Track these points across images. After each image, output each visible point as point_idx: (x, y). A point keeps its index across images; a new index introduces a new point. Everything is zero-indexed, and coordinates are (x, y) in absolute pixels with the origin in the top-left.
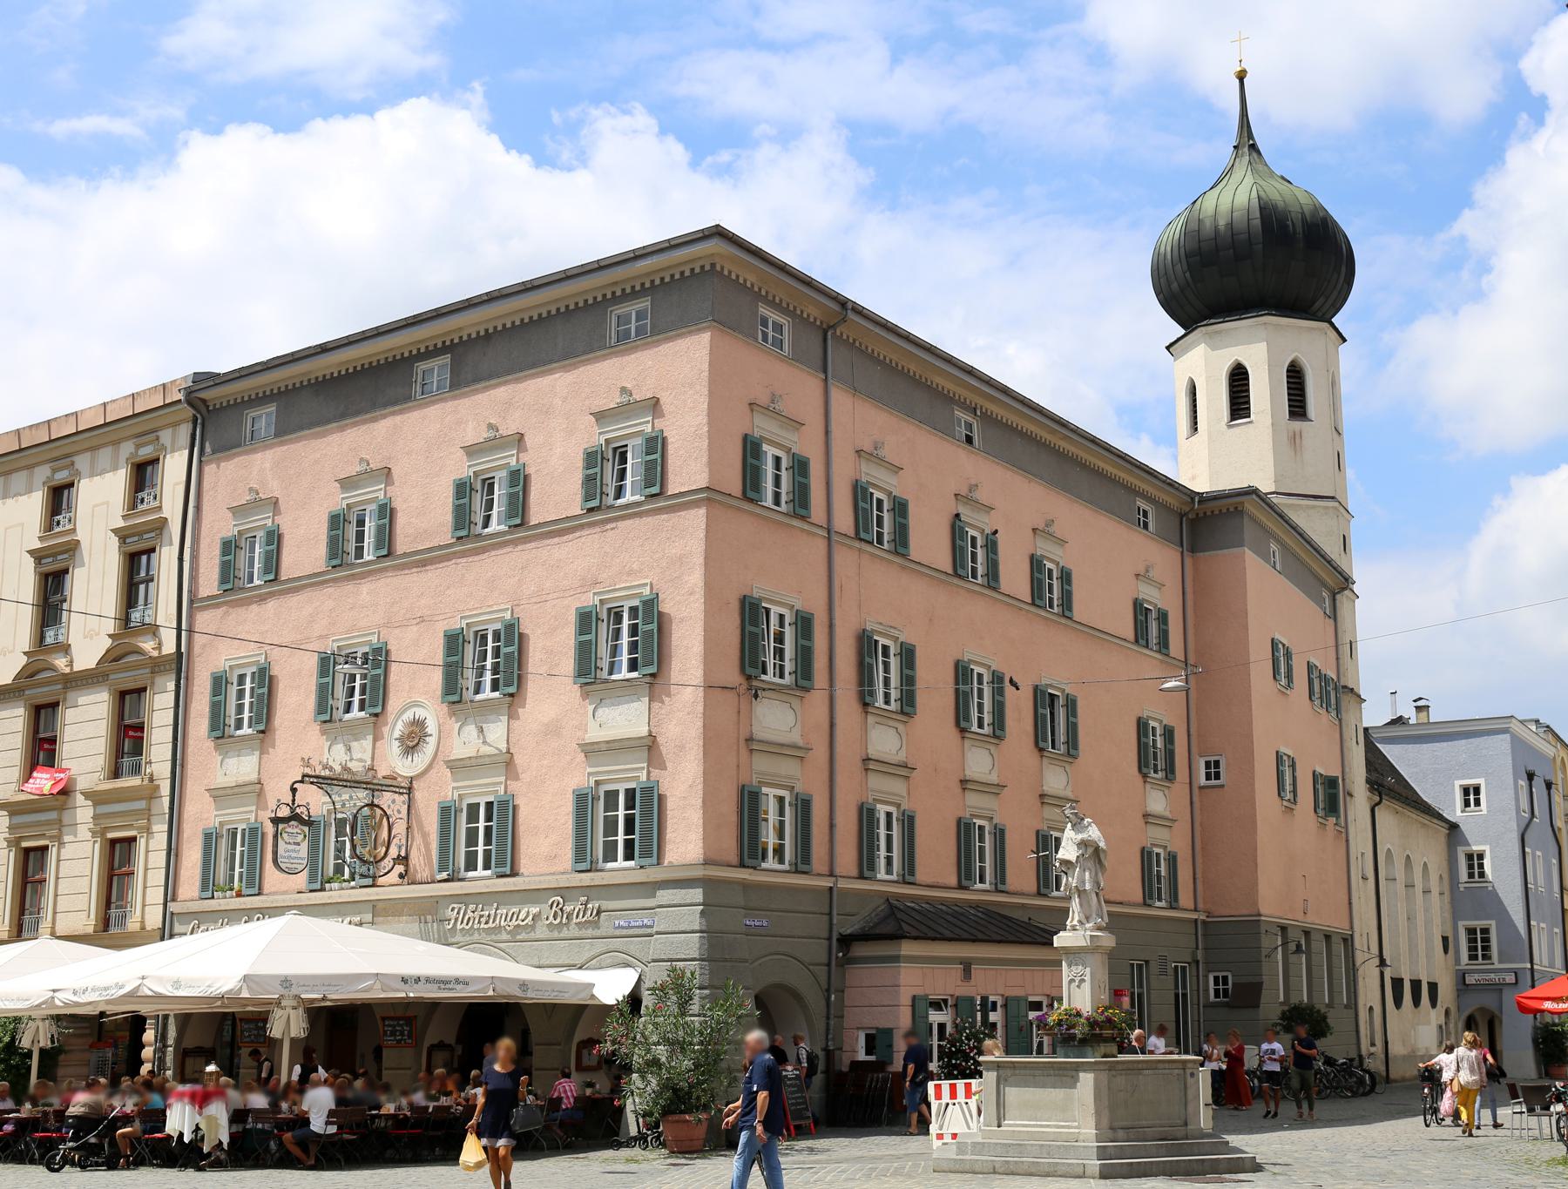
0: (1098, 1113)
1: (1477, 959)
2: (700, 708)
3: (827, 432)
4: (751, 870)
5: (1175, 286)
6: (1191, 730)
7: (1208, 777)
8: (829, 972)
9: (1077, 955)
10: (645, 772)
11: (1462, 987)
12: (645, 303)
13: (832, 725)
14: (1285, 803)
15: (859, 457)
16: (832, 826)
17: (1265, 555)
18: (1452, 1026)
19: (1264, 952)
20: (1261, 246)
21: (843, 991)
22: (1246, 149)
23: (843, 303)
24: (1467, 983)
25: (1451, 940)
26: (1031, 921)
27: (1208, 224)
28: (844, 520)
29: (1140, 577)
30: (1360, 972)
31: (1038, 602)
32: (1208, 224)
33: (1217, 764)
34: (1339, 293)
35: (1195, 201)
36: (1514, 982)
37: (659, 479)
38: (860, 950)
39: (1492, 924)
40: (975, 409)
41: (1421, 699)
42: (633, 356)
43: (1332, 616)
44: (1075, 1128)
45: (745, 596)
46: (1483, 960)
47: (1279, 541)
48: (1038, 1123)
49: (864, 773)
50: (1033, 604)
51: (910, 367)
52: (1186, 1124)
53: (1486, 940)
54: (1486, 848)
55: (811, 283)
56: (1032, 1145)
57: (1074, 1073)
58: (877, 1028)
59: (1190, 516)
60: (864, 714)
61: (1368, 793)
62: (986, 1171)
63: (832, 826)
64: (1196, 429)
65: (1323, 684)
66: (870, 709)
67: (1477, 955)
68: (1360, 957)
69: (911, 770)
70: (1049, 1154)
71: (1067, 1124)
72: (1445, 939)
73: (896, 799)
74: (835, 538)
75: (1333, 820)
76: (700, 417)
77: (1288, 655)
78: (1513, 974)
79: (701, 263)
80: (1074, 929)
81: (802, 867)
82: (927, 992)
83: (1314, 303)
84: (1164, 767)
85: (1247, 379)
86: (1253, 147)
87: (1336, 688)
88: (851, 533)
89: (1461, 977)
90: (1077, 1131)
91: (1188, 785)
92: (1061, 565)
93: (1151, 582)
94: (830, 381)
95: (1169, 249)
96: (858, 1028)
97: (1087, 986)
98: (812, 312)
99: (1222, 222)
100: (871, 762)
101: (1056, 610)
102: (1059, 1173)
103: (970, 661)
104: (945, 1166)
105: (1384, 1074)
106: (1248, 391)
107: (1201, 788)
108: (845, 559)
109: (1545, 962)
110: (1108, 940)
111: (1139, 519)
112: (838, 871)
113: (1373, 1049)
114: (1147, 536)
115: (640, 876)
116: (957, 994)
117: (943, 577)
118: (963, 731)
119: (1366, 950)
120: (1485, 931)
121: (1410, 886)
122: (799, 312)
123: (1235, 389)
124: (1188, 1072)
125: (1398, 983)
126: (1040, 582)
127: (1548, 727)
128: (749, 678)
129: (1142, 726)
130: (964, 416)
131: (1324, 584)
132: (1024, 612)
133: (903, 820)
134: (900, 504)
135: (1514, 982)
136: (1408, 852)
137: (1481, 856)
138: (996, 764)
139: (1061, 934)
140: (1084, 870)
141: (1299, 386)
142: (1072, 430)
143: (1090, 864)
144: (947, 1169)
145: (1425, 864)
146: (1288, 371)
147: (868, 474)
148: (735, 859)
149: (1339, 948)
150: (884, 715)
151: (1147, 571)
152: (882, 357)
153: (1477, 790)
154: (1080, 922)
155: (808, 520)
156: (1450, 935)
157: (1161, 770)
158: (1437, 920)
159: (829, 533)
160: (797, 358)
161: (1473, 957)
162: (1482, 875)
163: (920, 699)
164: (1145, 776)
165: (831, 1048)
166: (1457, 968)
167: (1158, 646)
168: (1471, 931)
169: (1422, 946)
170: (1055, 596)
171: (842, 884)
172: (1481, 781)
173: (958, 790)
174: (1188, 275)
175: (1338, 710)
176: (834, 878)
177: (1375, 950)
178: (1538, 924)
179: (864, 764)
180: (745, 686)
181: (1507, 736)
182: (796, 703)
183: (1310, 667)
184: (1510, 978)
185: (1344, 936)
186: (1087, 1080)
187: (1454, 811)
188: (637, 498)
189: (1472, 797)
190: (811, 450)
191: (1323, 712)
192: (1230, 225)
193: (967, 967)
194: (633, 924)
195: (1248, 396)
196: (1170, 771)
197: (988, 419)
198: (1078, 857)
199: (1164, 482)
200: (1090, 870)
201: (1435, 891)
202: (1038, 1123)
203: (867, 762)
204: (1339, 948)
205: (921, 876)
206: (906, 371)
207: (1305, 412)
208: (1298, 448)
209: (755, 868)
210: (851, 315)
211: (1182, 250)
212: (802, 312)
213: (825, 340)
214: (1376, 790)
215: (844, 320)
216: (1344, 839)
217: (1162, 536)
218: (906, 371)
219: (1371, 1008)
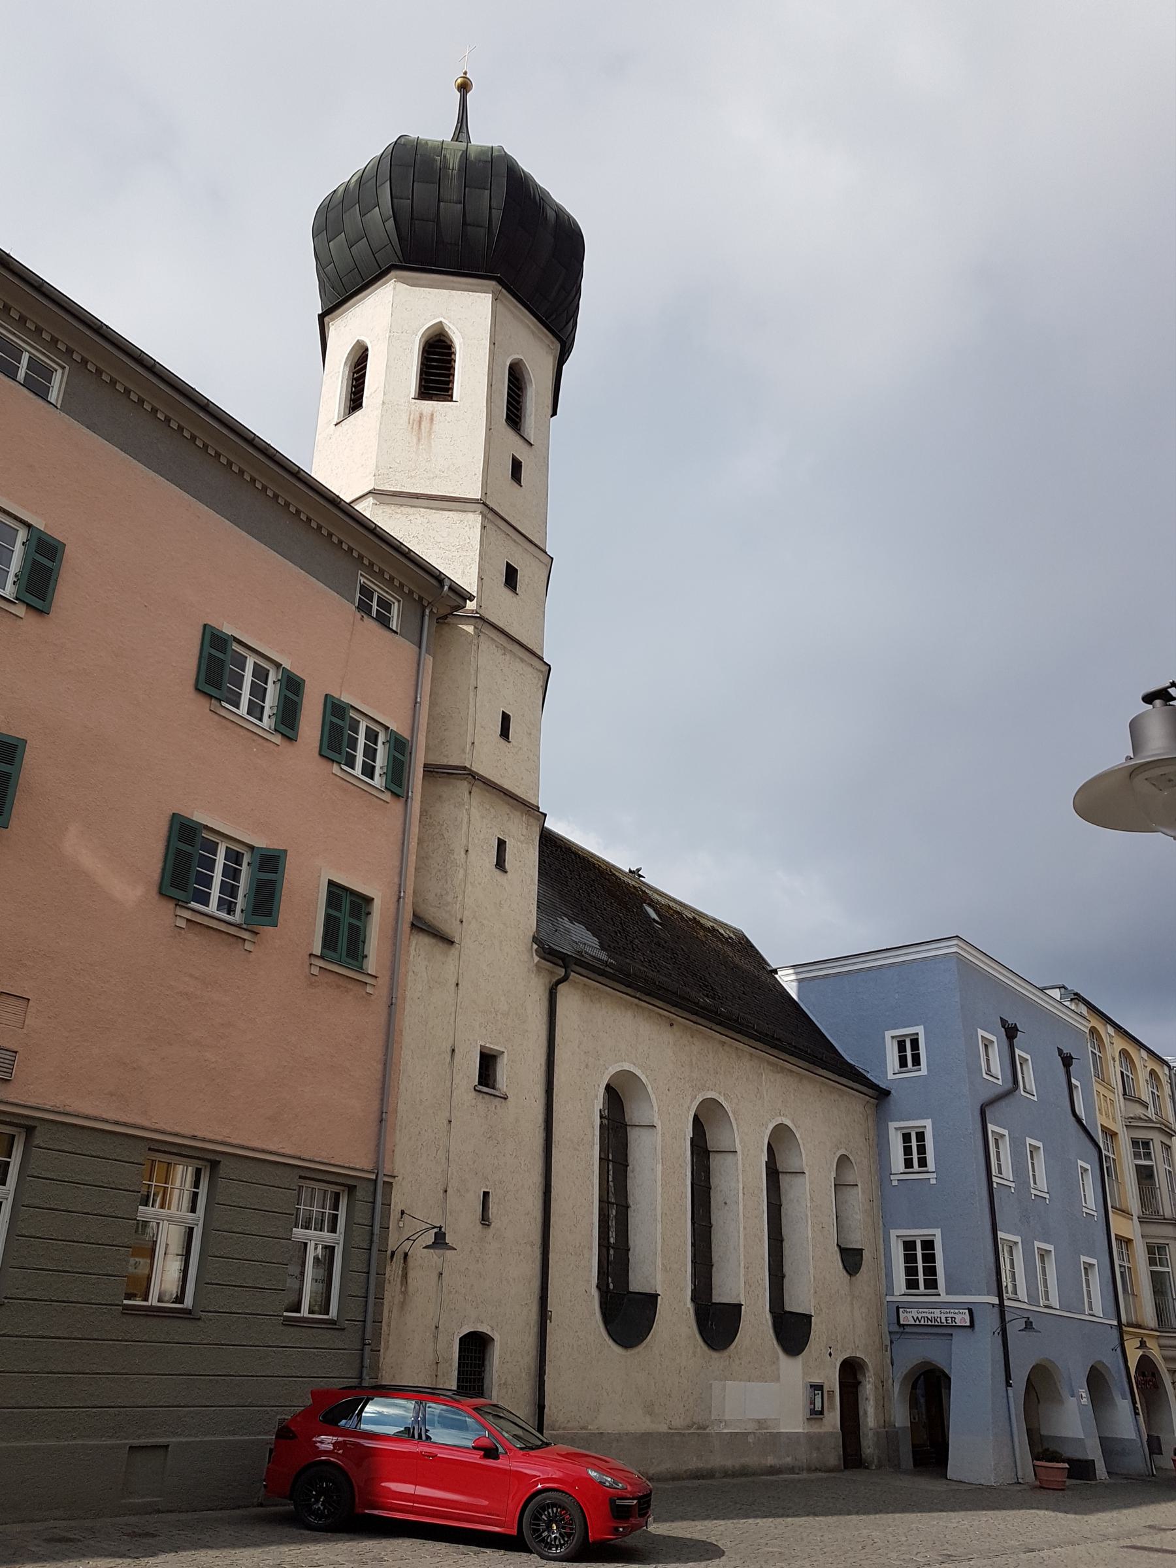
11: (896, 1328)
24: (902, 1322)
53: (929, 1258)
61: (536, 959)
109: (1022, 1294)
120: (928, 1245)
161: (912, 1284)
162: (923, 1162)
166: (889, 1298)
168: (909, 1245)
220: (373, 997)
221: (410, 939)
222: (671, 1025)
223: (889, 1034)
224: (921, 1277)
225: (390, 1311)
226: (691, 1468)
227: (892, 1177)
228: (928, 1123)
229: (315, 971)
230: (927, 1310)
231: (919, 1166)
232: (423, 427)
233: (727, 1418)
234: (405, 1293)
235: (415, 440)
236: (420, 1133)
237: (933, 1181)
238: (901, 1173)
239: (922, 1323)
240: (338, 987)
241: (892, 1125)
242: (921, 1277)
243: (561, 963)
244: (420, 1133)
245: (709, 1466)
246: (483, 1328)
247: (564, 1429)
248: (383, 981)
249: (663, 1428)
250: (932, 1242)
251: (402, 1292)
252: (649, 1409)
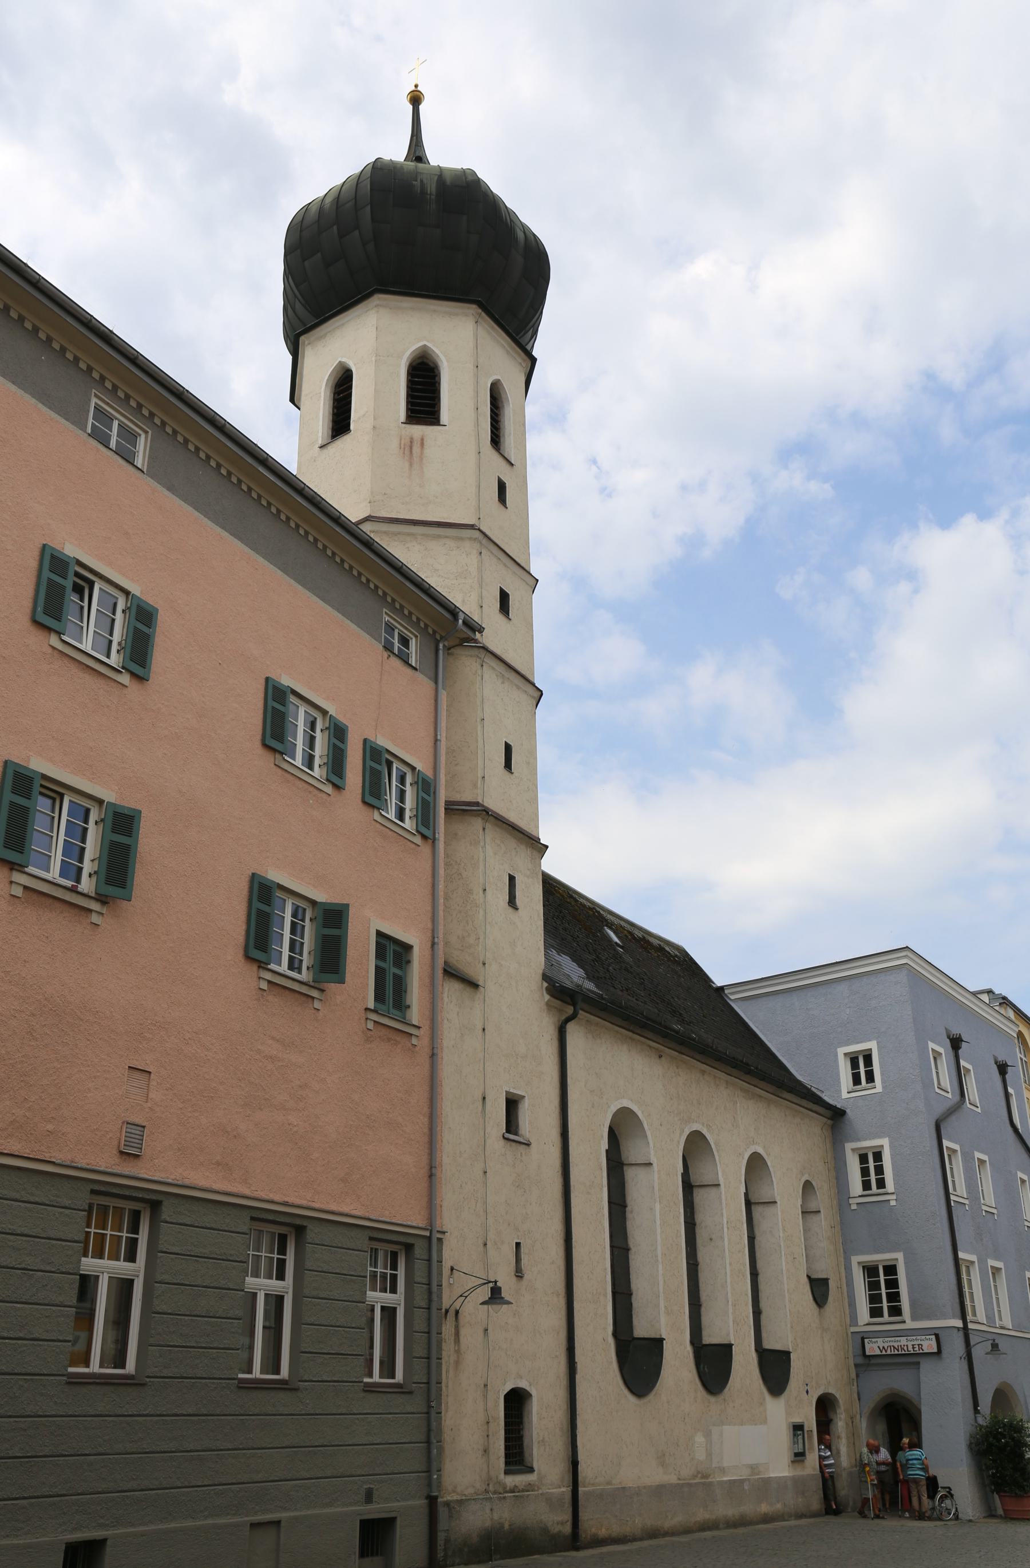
1: (882, 1316)
24: (868, 1353)
36: (935, 1350)
46: (890, 1315)
53: (892, 1284)
54: (884, 1143)
61: (547, 997)
78: (933, 1337)
120: (891, 1270)
127: (1004, 998)
135: (935, 1350)
137: (878, 1156)
153: (868, 1059)
161: (875, 1312)
162: (881, 1183)
166: (854, 1329)
168: (870, 1271)
172: (872, 1045)
178: (982, 1261)
181: (902, 976)
184: (929, 1345)
187: (840, 1091)
189: (862, 1070)
220: (417, 1049)
221: (443, 985)
222: (660, 1057)
223: (841, 1051)
224: (885, 1304)
225: (447, 1372)
226: (699, 1519)
227: (851, 1201)
228: (885, 1142)
229: (370, 1025)
230: (893, 1339)
231: (878, 1188)
232: (414, 451)
233: (725, 1464)
234: (458, 1352)
235: (407, 465)
236: (461, 1186)
237: (893, 1203)
238: (860, 1196)
239: (889, 1352)
240: (389, 1040)
241: (849, 1146)
242: (885, 1304)
243: (569, 1000)
244: (461, 1186)
245: (714, 1517)
246: (523, 1384)
247: (593, 1485)
248: (425, 1032)
249: (673, 1479)
251: (455, 1351)
252: (662, 1460)
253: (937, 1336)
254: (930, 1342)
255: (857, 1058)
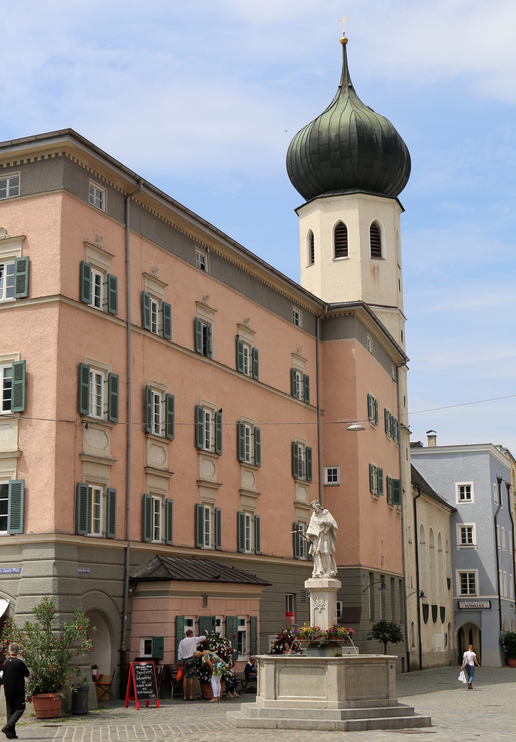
0: (339, 691)
2: (53, 434)
3: (126, 261)
4: (82, 537)
5: (302, 172)
6: (320, 450)
7: (330, 479)
8: (124, 601)
9: (319, 593)
10: (15, 474)
11: (457, 610)
12: (18, 174)
13: (128, 446)
14: (373, 496)
15: (144, 277)
16: (127, 509)
17: (365, 343)
18: (451, 634)
19: (363, 589)
20: (357, 150)
21: (131, 613)
22: (347, 89)
23: (138, 180)
24: (460, 607)
25: (451, 580)
26: (234, 569)
27: (324, 134)
28: (136, 318)
29: (294, 355)
30: (408, 601)
31: (240, 370)
32: (324, 134)
33: (335, 471)
34: (402, 181)
35: (317, 119)
36: (489, 607)
37: (26, 288)
38: (143, 588)
39: (476, 571)
40: (207, 249)
41: (431, 431)
42: (8, 208)
43: (396, 380)
44: (325, 700)
45: (80, 364)
46: (470, 593)
47: (372, 335)
48: (301, 697)
49: (145, 476)
50: (237, 371)
51: (172, 221)
52: (388, 697)
53: (472, 581)
54: (474, 524)
55: (121, 167)
56: (299, 711)
57: (324, 666)
58: (153, 637)
59: (321, 318)
60: (145, 439)
61: (412, 490)
62: (271, 727)
63: (127, 509)
64: (313, 262)
65: (392, 423)
66: (149, 436)
67: (467, 590)
68: (408, 591)
69: (170, 474)
70: (310, 716)
71: (319, 697)
72: (449, 580)
73: (162, 492)
74: (131, 328)
75: (395, 506)
76: (55, 250)
77: (376, 405)
79: (56, 152)
80: (317, 577)
81: (110, 535)
82: (184, 614)
83: (386, 188)
84: (305, 473)
85: (346, 232)
86: (351, 87)
87: (397, 426)
88: (139, 325)
89: (457, 603)
90: (326, 702)
91: (318, 484)
92: (252, 347)
93: (299, 357)
94: (128, 229)
95: (299, 148)
96: (140, 637)
97: (326, 612)
98: (119, 185)
99: (333, 134)
100: (150, 469)
101: (249, 374)
102: (319, 728)
103: (203, 406)
104: (245, 724)
105: (419, 664)
106: (346, 239)
107: (325, 486)
108: (136, 341)
109: (506, 596)
110: (338, 584)
111: (294, 318)
112: (130, 538)
113: (413, 649)
114: (298, 329)
115: (12, 541)
116: (199, 615)
117: (189, 353)
118: (199, 449)
119: (411, 587)
120: (472, 575)
121: (432, 547)
122: (111, 185)
123: (338, 238)
124: (390, 665)
125: (426, 607)
126: (241, 357)
127: (507, 450)
128: (82, 415)
129: (294, 448)
130: (200, 252)
131: (392, 361)
132: (232, 376)
133: (166, 506)
134: (166, 307)
135: (489, 607)
136: (431, 526)
137: (470, 529)
138: (216, 471)
139: (310, 580)
140: (324, 541)
141: (377, 238)
142: (260, 263)
143: (327, 537)
144: (246, 726)
145: (439, 533)
146: (371, 228)
147: (148, 288)
148: (72, 530)
149: (397, 586)
150: (157, 439)
151: (298, 351)
152: (156, 215)
153: (468, 488)
154: (321, 572)
155: (116, 316)
156: (451, 578)
157: (304, 475)
158: (445, 568)
159: (127, 325)
160: (110, 214)
161: (464, 591)
162: (470, 541)
163: (177, 429)
164: (295, 478)
165: (124, 650)
166: (455, 598)
167: (303, 398)
168: (463, 576)
169: (437, 584)
170: (248, 366)
171: (133, 546)
172: (471, 483)
173: (195, 487)
174: (311, 165)
175: (398, 438)
176: (127, 543)
177: (415, 586)
178: (502, 572)
179: (145, 470)
180: (79, 421)
181: (487, 456)
182: (108, 431)
183: (386, 412)
184: (487, 605)
185: (401, 579)
186: (332, 670)
187: (455, 501)
188: (11, 299)
189: (465, 493)
190: (118, 273)
191: (391, 439)
192: (338, 136)
193: (205, 597)
194: (5, 571)
195: (346, 243)
196: (309, 475)
197: (214, 255)
198: (320, 533)
199: (309, 296)
200: (327, 541)
201: (444, 550)
202: (301, 697)
203: (147, 469)
204: (397, 586)
205: (176, 541)
206: (169, 223)
207: (381, 254)
208: (376, 276)
209: (83, 535)
210: (142, 188)
211: (308, 150)
212: (113, 184)
213: (126, 203)
214: (417, 488)
215: (138, 191)
216: (401, 518)
217: (306, 330)
218: (169, 223)
219: (413, 623)
224: (468, 589)
227: (457, 547)
230: (471, 602)
232: (375, 273)
238: (460, 545)
239: (469, 607)
241: (458, 525)
242: (468, 589)
250: (474, 574)
253: (490, 602)
254: (487, 604)
255: (463, 487)
